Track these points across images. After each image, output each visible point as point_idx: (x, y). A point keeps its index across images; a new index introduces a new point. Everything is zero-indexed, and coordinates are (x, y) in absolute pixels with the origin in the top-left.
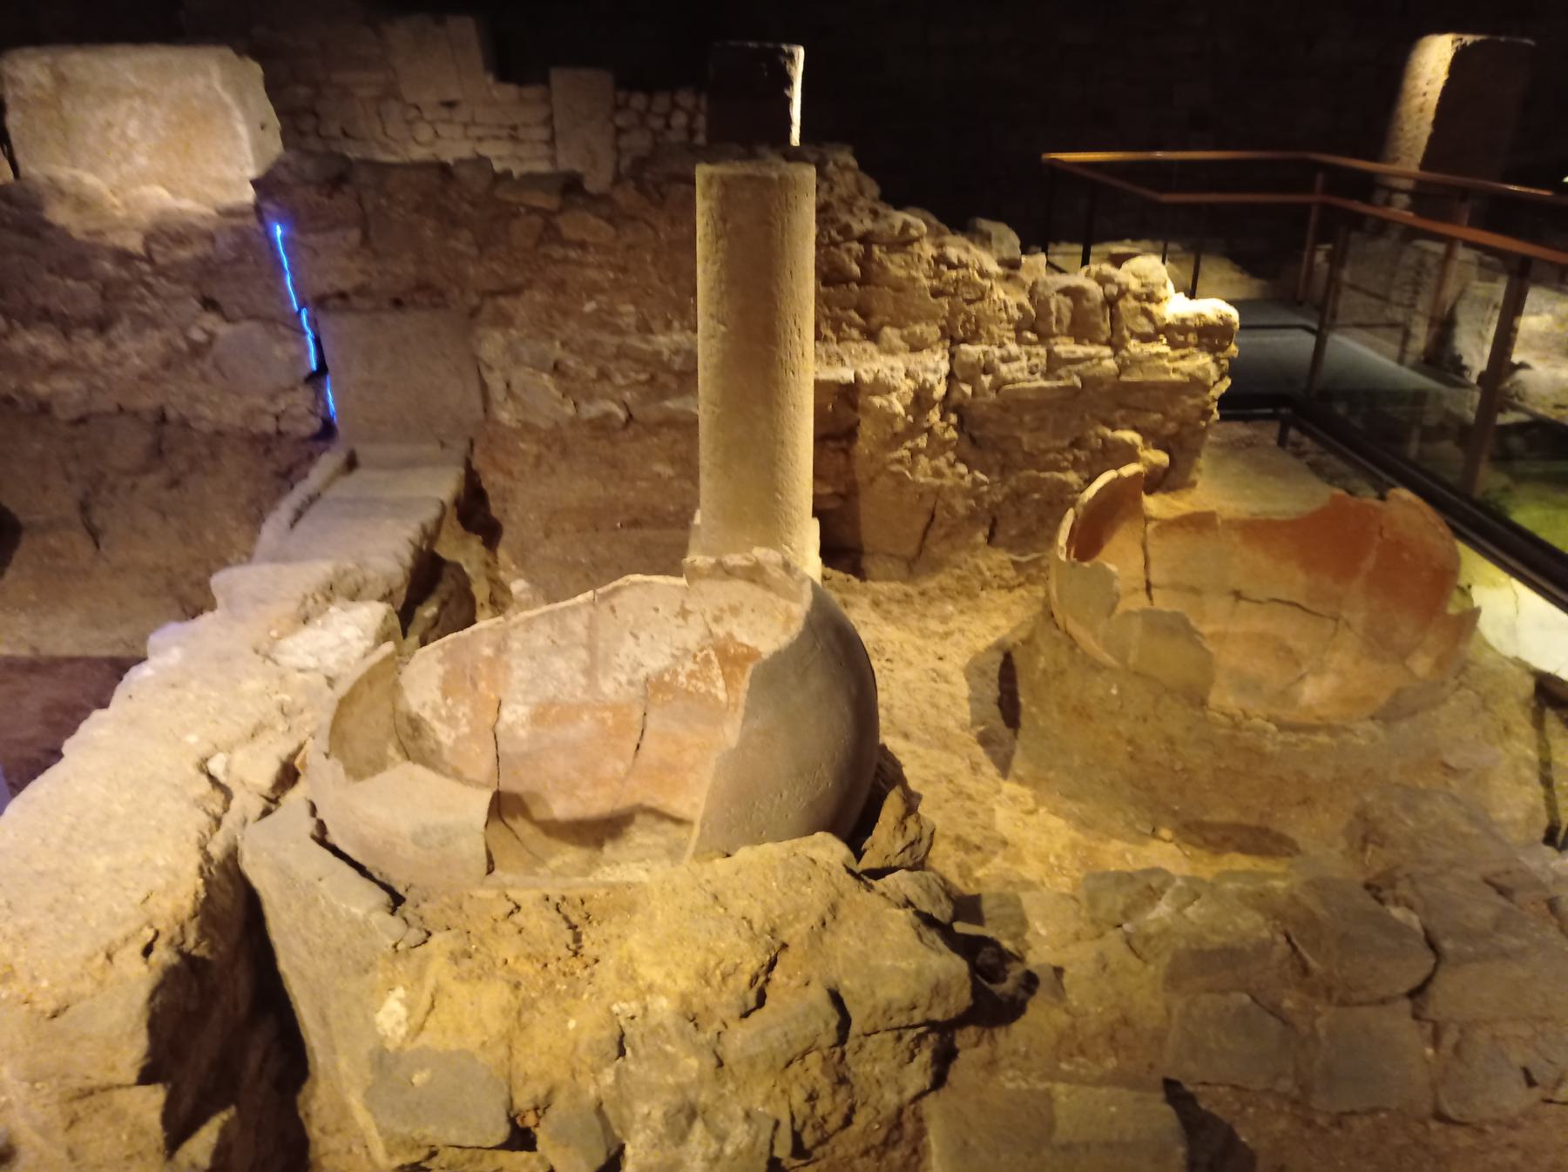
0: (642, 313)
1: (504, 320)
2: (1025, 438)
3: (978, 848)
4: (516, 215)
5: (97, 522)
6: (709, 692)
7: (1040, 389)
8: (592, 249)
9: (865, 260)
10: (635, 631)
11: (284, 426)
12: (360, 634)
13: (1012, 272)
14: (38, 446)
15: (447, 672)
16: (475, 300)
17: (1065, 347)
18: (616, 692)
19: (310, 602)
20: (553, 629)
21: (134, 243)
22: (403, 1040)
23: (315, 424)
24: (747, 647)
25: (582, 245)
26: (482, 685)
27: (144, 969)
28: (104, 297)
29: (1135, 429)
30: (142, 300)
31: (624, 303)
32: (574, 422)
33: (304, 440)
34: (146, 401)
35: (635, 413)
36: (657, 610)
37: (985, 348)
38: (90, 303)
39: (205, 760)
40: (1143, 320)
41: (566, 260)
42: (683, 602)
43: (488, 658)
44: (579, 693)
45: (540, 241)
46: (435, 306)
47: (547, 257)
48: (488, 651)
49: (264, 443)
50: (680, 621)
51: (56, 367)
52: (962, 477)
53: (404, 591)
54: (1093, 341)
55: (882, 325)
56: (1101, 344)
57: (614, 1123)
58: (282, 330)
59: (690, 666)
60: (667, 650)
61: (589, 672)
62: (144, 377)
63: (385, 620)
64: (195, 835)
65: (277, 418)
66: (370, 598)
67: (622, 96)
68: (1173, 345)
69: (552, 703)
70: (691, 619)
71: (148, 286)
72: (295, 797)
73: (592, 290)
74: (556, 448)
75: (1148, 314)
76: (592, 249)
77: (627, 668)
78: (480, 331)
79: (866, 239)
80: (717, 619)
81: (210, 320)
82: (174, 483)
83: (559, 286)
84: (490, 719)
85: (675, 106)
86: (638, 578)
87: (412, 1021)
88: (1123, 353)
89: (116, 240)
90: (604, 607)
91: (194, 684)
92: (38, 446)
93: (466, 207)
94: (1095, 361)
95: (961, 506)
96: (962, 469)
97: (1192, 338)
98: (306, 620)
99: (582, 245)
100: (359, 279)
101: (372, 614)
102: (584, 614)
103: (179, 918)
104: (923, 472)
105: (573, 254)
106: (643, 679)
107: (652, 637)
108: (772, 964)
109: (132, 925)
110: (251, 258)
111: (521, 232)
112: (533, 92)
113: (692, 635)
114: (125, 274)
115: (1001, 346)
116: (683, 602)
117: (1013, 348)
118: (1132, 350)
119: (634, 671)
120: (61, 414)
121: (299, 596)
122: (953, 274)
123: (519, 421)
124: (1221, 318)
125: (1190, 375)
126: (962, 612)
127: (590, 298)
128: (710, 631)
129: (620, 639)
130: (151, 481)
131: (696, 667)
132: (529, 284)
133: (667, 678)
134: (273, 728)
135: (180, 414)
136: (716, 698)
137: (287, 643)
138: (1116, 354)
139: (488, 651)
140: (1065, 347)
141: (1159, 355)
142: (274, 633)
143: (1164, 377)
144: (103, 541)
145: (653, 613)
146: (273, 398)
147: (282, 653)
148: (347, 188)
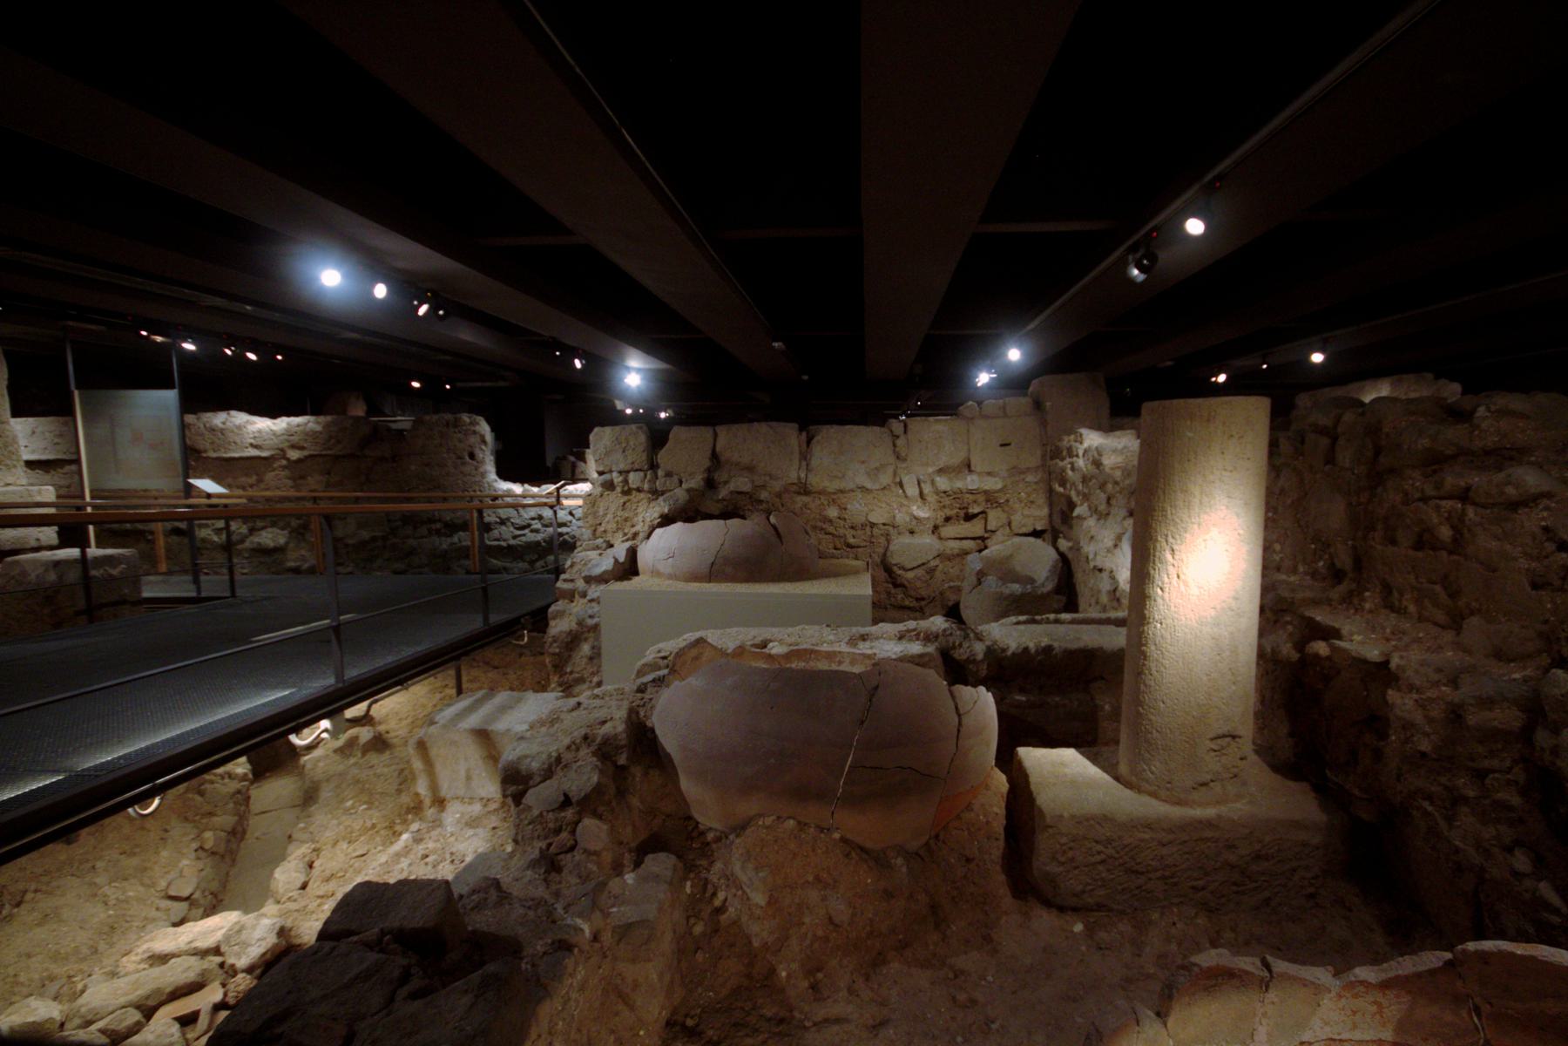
21: (1118, 474)
52: (1516, 874)
62: (1109, 551)
79: (1464, 496)
96: (1521, 862)
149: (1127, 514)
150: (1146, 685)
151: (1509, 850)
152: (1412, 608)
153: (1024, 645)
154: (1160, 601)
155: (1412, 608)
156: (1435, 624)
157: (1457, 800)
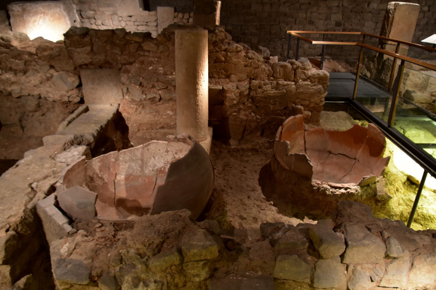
2: (271, 107)
3: (245, 219)
4: (131, 43)
5: (23, 125)
7: (274, 93)
8: (151, 53)
9: (226, 56)
10: (154, 156)
11: (70, 100)
12: (78, 154)
13: (267, 61)
14: (9, 104)
15: (101, 165)
16: (120, 66)
17: (282, 82)
18: (149, 173)
19: (66, 145)
20: (131, 155)
21: (33, 50)
22: (66, 256)
23: (78, 99)
25: (149, 51)
26: (111, 169)
27: (5, 235)
28: (25, 64)
29: (302, 105)
30: (35, 66)
31: (160, 67)
32: (145, 100)
33: (76, 103)
34: (36, 92)
35: (162, 96)
36: (160, 150)
37: (259, 81)
38: (22, 66)
39: (31, 184)
41: (144, 55)
43: (113, 162)
44: (138, 173)
45: (137, 50)
46: (111, 68)
47: (139, 54)
48: (113, 160)
49: (66, 104)
50: (166, 153)
51: (13, 83)
52: (253, 117)
53: (94, 144)
54: (289, 80)
55: (231, 74)
56: (292, 81)
57: (119, 281)
58: (70, 74)
61: (142, 167)
62: (35, 86)
63: (86, 150)
64: (24, 202)
65: (69, 97)
66: (84, 145)
68: (311, 81)
69: (131, 175)
70: (169, 153)
71: (36, 62)
72: (53, 196)
73: (151, 63)
74: (141, 107)
75: (304, 73)
76: (151, 53)
77: (152, 167)
78: (121, 74)
79: (225, 50)
80: (176, 153)
81: (52, 71)
82: (43, 115)
83: (142, 63)
84: (113, 179)
85: (190, 17)
87: (69, 252)
88: (298, 83)
89: (28, 50)
90: (146, 149)
91: (33, 165)
92: (9, 104)
93: (118, 41)
94: (290, 86)
95: (253, 125)
96: (253, 114)
97: (316, 80)
98: (65, 150)
99: (149, 51)
100: (90, 60)
101: (82, 148)
102: (140, 150)
103: (16, 223)
104: (242, 116)
105: (146, 54)
106: (156, 169)
107: (159, 158)
108: (163, 242)
109: (4, 224)
110: (62, 55)
111: (132, 48)
112: (152, 13)
114: (31, 59)
115: (264, 81)
116: (167, 148)
117: (267, 81)
118: (300, 83)
119: (154, 167)
120: (15, 95)
121: (64, 143)
122: (250, 60)
124: (324, 75)
126: (253, 155)
127: (151, 65)
128: (174, 157)
129: (150, 158)
130: (37, 114)
132: (134, 62)
133: (163, 169)
134: (50, 176)
135: (44, 96)
137: (59, 155)
138: (295, 84)
139: (113, 160)
140: (282, 82)
141: (308, 85)
142: (56, 153)
143: (309, 91)
144: (25, 129)
145: (159, 151)
146: (68, 92)
147: (57, 158)
148: (87, 36)
149: (49, 68)
150: (198, 113)
151: (250, 114)
152: (216, 76)
153: (96, 130)
154: (201, 89)
155: (216, 76)
156: (223, 78)
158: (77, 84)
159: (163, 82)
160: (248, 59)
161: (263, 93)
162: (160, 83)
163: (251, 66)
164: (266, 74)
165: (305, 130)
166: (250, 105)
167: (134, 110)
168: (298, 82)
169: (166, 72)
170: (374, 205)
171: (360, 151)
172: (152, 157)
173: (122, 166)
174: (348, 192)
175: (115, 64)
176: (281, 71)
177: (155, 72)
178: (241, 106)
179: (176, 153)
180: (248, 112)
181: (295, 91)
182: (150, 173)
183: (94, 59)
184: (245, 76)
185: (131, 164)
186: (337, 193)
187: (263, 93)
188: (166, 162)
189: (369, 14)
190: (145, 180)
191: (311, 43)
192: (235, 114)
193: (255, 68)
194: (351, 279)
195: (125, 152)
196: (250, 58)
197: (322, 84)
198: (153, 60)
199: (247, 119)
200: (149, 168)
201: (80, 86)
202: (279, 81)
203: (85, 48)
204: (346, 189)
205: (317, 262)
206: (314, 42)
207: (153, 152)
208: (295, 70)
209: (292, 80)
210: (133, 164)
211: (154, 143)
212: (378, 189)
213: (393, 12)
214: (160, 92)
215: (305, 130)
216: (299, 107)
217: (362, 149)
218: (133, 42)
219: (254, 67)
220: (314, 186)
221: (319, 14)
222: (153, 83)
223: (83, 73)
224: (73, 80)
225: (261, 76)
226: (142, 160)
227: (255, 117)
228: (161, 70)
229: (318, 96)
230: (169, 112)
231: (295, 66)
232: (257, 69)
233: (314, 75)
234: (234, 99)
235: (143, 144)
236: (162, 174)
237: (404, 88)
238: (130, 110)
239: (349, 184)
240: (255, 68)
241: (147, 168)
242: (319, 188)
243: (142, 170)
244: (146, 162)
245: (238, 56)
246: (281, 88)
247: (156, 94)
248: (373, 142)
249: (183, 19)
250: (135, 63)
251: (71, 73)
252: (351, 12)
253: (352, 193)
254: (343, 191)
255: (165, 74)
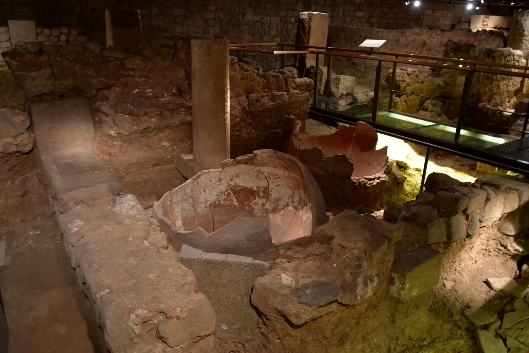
0: (154, 92)
1: (106, 99)
2: (267, 121)
6: (231, 204)
10: (205, 190)
16: (95, 92)
17: (276, 93)
18: (202, 211)
24: (242, 186)
25: (133, 70)
29: (293, 115)
31: (148, 89)
36: (211, 181)
40: (293, 84)
41: (128, 75)
42: (220, 176)
44: (192, 214)
48: (169, 203)
50: (219, 183)
54: (282, 91)
56: (284, 91)
59: (224, 197)
60: (215, 193)
61: (193, 206)
67: (39, 30)
70: (222, 181)
75: (294, 82)
80: (231, 180)
83: (126, 85)
85: (61, 33)
86: (205, 171)
90: (195, 183)
93: (92, 59)
96: (254, 131)
97: (304, 88)
99: (133, 70)
100: (52, 88)
102: (190, 185)
105: (131, 73)
106: (209, 205)
113: (223, 187)
116: (220, 176)
118: (292, 92)
119: (206, 203)
123: (117, 133)
125: (305, 98)
127: (136, 88)
128: (229, 184)
129: (200, 193)
131: (225, 197)
132: (114, 85)
133: (217, 203)
136: (234, 205)
138: (288, 94)
140: (276, 93)
141: (298, 93)
143: (299, 99)
146: (15, 137)
157: (242, 127)
158: (28, 124)
159: (156, 107)
160: (243, 71)
161: (262, 106)
162: (153, 109)
163: (247, 79)
164: (261, 86)
165: (300, 140)
166: (250, 121)
167: (118, 148)
168: (289, 91)
169: (156, 94)
170: (397, 188)
171: (350, 150)
172: (202, 191)
173: (176, 210)
174: (381, 181)
175: (88, 89)
176: (274, 82)
177: (142, 95)
178: (243, 124)
179: (231, 180)
180: (249, 129)
181: (288, 101)
182: (204, 210)
183: (56, 85)
184: (242, 91)
185: (183, 205)
186: (374, 184)
187: (262, 106)
188: (219, 194)
189: (245, 26)
190: (201, 221)
191: (273, 53)
192: (238, 133)
193: (251, 81)
194: (470, 225)
195: (177, 191)
196: (246, 71)
197: (309, 92)
198: (139, 80)
199: (249, 137)
200: (201, 205)
201: (31, 128)
202: (273, 92)
203: (43, 71)
204: (378, 178)
205: (449, 220)
206: (275, 52)
207: (203, 184)
208: (286, 79)
209: (284, 89)
210: (185, 205)
211: (205, 173)
212: (396, 174)
213: (308, 21)
214: (153, 119)
215: (300, 140)
216: (293, 117)
217: (351, 147)
218: (112, 59)
219: (250, 79)
220: (356, 183)
221: (196, 27)
222: (145, 109)
223: (36, 109)
224: (20, 119)
225: (257, 88)
226: (192, 198)
227: (255, 134)
228: (149, 93)
229: (306, 104)
230: (164, 143)
231: (286, 75)
232: (253, 82)
233: (302, 83)
234: (238, 117)
235: (191, 178)
236: (217, 208)
237: (338, 93)
238: (111, 149)
239: (378, 174)
240: (251, 81)
241: (199, 206)
242: (360, 183)
243: (195, 211)
244: (197, 199)
245: (234, 69)
246: (277, 100)
247: (150, 122)
248: (362, 138)
249: (51, 37)
250: (114, 86)
251: (18, 109)
252: (228, 24)
253: (384, 181)
254: (377, 181)
255: (156, 96)
